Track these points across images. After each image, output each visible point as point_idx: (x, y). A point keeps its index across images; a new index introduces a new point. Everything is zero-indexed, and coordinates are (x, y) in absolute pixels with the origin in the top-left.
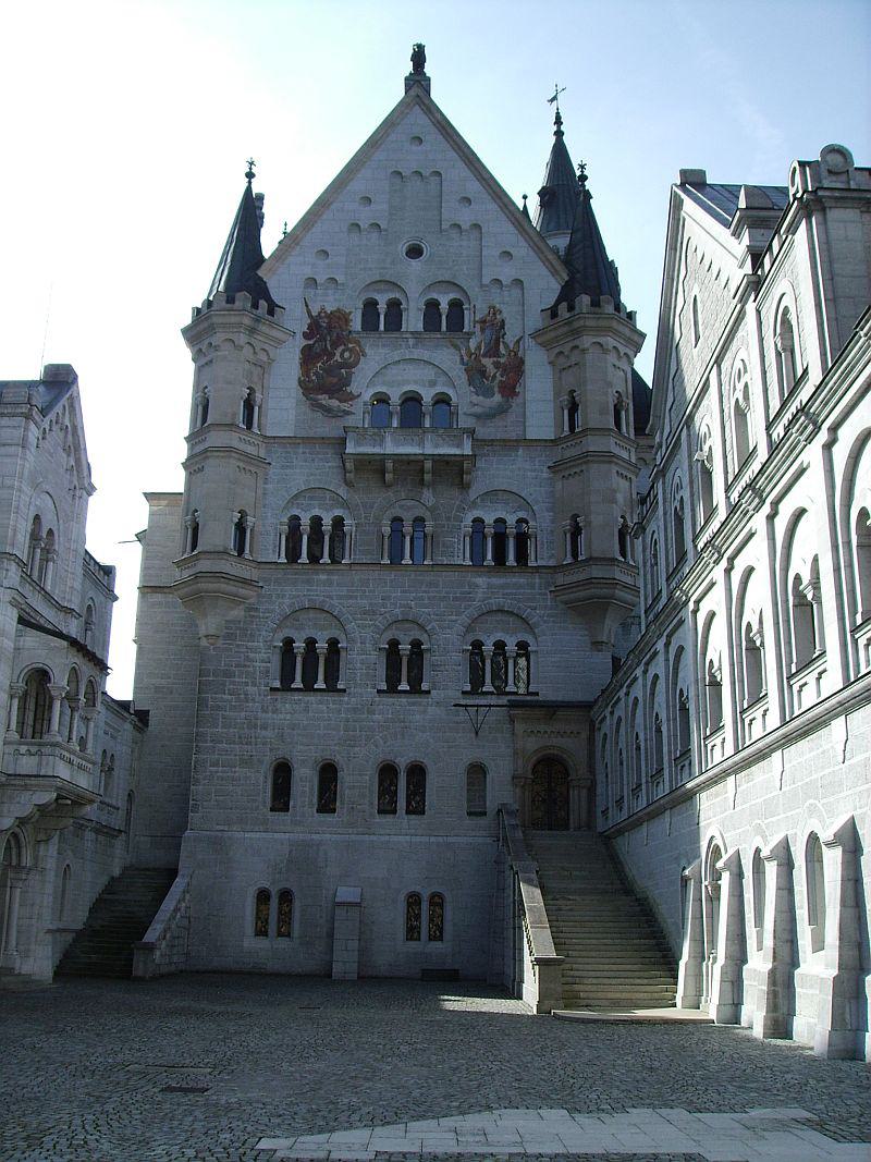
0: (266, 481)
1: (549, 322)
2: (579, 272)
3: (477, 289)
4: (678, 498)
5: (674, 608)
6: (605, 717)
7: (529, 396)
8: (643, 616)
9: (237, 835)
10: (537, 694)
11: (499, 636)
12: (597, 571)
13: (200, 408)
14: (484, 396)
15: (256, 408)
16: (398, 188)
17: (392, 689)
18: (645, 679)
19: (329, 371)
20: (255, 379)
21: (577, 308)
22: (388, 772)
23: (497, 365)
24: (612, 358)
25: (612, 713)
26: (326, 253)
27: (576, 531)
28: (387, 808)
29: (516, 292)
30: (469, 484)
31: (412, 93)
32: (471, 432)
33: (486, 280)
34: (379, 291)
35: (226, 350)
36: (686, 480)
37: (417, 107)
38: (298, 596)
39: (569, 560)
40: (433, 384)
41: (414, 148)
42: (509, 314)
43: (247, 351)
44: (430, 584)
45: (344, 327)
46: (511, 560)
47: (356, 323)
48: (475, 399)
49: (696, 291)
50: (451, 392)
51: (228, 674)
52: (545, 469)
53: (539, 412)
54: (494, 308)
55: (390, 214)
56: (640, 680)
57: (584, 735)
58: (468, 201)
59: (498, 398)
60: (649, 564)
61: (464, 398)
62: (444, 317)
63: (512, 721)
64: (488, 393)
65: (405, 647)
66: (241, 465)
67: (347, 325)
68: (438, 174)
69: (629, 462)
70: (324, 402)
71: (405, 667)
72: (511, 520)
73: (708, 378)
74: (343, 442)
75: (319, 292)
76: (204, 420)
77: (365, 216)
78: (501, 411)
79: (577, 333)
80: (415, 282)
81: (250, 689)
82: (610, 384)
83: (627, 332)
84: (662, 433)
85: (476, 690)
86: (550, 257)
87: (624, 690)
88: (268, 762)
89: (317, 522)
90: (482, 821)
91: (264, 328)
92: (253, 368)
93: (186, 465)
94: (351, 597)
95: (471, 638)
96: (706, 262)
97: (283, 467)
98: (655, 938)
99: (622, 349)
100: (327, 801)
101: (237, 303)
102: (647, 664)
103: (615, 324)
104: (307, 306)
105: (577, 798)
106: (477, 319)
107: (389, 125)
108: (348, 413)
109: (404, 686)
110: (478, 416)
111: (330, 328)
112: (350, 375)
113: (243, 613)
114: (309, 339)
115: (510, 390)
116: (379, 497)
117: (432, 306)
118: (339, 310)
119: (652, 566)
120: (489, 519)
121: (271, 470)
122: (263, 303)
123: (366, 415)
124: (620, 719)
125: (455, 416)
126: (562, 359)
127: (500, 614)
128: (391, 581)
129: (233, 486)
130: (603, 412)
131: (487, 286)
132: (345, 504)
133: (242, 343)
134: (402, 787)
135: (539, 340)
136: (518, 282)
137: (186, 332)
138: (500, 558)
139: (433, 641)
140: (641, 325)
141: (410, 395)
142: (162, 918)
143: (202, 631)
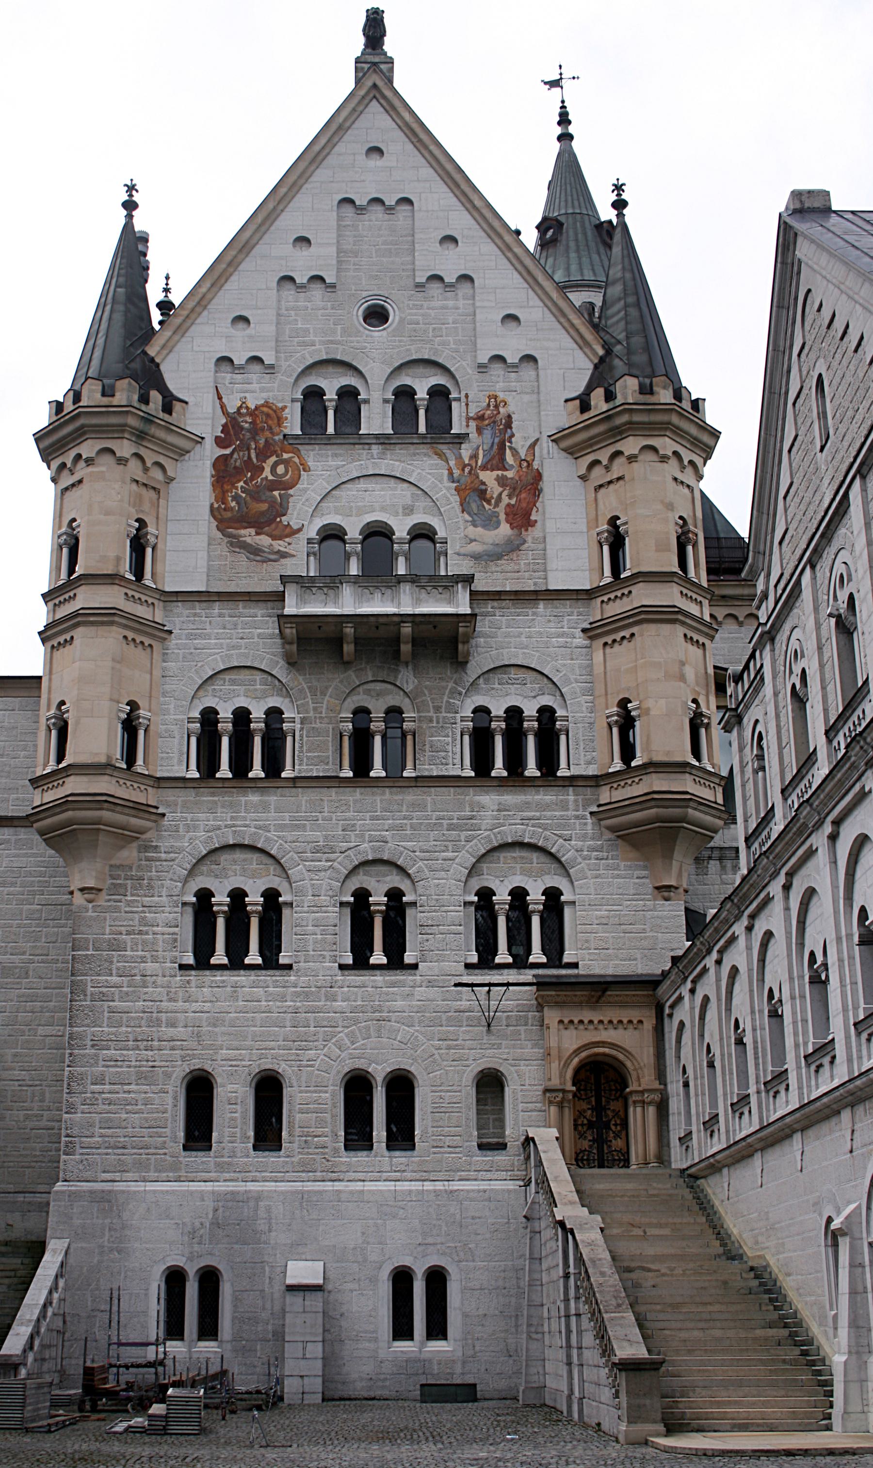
0: (165, 658)
1: (577, 417)
2: (619, 342)
4: (797, 670)
5: (800, 832)
6: (680, 998)
7: (550, 526)
8: (742, 845)
9: (133, 1187)
10: (575, 965)
11: (517, 881)
12: (658, 783)
13: (65, 551)
14: (484, 527)
15: (149, 551)
17: (361, 962)
18: (749, 939)
19: (255, 495)
20: (146, 506)
22: (357, 1087)
23: (502, 481)
24: (672, 468)
25: (692, 991)
26: (244, 319)
29: (528, 372)
30: (468, 654)
32: (468, 579)
33: (484, 358)
36: (810, 646)
37: (374, 102)
38: (219, 828)
39: (618, 765)
40: (409, 510)
42: (516, 406)
43: (134, 464)
44: (413, 806)
45: (276, 429)
46: (532, 769)
47: (293, 425)
48: (472, 531)
49: (821, 368)
50: (435, 522)
51: (116, 946)
52: (578, 632)
54: (496, 397)
55: (339, 262)
56: (742, 941)
57: (649, 1024)
58: (450, 239)
59: (505, 529)
60: (749, 769)
62: (422, 413)
63: (540, 1007)
64: (491, 522)
65: (378, 899)
66: (131, 635)
67: (279, 425)
68: (407, 201)
70: (248, 540)
71: (378, 930)
72: (530, 709)
73: (846, 495)
74: (280, 597)
76: (71, 570)
78: (512, 548)
79: (619, 433)
80: (377, 359)
81: (150, 967)
82: (670, 507)
83: (694, 431)
84: (768, 575)
86: (577, 321)
87: (714, 955)
88: (180, 1071)
89: (242, 716)
90: (500, 1158)
91: (161, 434)
92: (143, 491)
93: (45, 636)
94: (297, 827)
95: (476, 884)
96: (839, 326)
97: (190, 637)
98: (786, 1326)
99: (687, 455)
100: (268, 1132)
101: (118, 394)
102: (753, 917)
103: (675, 419)
104: (220, 398)
105: (641, 1121)
106: (471, 415)
107: (335, 129)
108: (284, 555)
109: (378, 957)
111: (255, 431)
112: (285, 498)
113: (135, 853)
114: (225, 447)
115: (522, 519)
116: (335, 681)
117: (405, 394)
118: (267, 404)
119: (755, 772)
120: (498, 709)
121: (173, 642)
122: (156, 397)
123: (312, 558)
124: (706, 999)
125: (442, 559)
126: (597, 471)
127: (517, 849)
128: (355, 802)
129: (118, 666)
130: (661, 547)
132: (284, 690)
133: (127, 456)
136: (529, 359)
137: (39, 438)
138: (515, 762)
139: (420, 891)
140: (712, 417)
142: (28, 1317)
143: (76, 885)
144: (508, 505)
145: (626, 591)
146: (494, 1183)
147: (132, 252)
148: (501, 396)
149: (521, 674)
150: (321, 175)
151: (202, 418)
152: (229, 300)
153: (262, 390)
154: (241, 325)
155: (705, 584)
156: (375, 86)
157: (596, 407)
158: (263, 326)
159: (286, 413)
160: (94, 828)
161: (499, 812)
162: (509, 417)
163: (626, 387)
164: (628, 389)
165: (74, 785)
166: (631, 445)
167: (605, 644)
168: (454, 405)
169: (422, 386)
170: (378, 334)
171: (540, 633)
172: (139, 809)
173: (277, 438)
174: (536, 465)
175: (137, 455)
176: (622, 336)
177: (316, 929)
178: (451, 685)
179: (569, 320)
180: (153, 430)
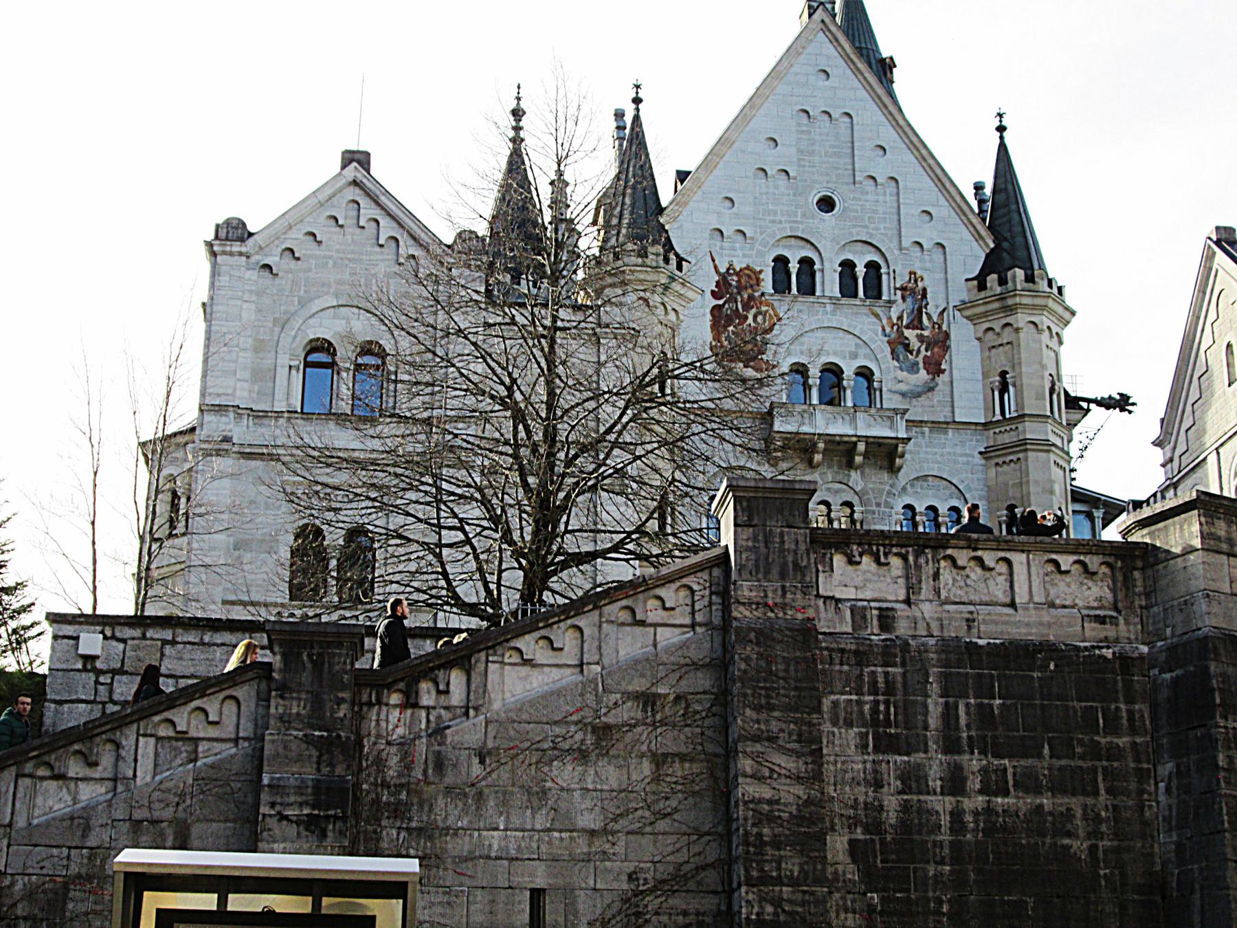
1: (976, 295)
3: (897, 252)
16: (804, 128)
21: (1010, 284)
23: (921, 338)
31: (815, 16)
32: (905, 411)
34: (789, 247)
37: (821, 34)
40: (854, 356)
41: (821, 83)
42: (931, 282)
43: (660, 311)
47: (767, 285)
50: (873, 366)
55: (799, 160)
59: (923, 373)
61: (888, 372)
62: (860, 282)
64: (913, 368)
69: (1062, 450)
75: (726, 245)
79: (1011, 310)
82: (1043, 367)
83: (1060, 310)
84: (1175, 448)
99: (1055, 329)
103: (1051, 303)
106: (898, 285)
107: (793, 51)
110: (903, 395)
115: (935, 368)
117: (848, 267)
118: (748, 268)
122: (672, 256)
131: (907, 249)
135: (968, 313)
141: (834, 368)
144: (926, 356)
145: (1013, 427)
148: (919, 273)
149: (937, 482)
150: (782, 88)
153: (744, 256)
154: (728, 204)
155: (1064, 423)
156: (823, 21)
157: (991, 289)
159: (761, 276)
162: (924, 290)
163: (1014, 277)
166: (1021, 319)
167: (997, 464)
168: (884, 277)
171: (949, 453)
173: (756, 294)
174: (944, 327)
175: (663, 304)
176: (1008, 235)
178: (888, 488)
179: (968, 219)
180: (676, 286)
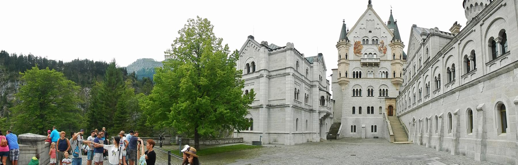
12: (397, 79)
17: (369, 96)
22: (368, 108)
27: (394, 74)
28: (368, 112)
35: (343, 48)
47: (362, 43)
53: (389, 56)
65: (370, 90)
71: (370, 93)
77: (362, 27)
79: (395, 45)
85: (380, 96)
89: (357, 72)
115: (385, 53)
117: (373, 40)
134: (370, 110)
140: (404, 44)
146: (381, 117)
147: (344, 26)
151: (352, 42)
152: (355, 31)
158: (358, 33)
160: (343, 83)
161: (382, 82)
164: (396, 40)
165: (342, 79)
166: (396, 46)
169: (375, 39)
170: (370, 34)
172: (348, 81)
177: (365, 93)
